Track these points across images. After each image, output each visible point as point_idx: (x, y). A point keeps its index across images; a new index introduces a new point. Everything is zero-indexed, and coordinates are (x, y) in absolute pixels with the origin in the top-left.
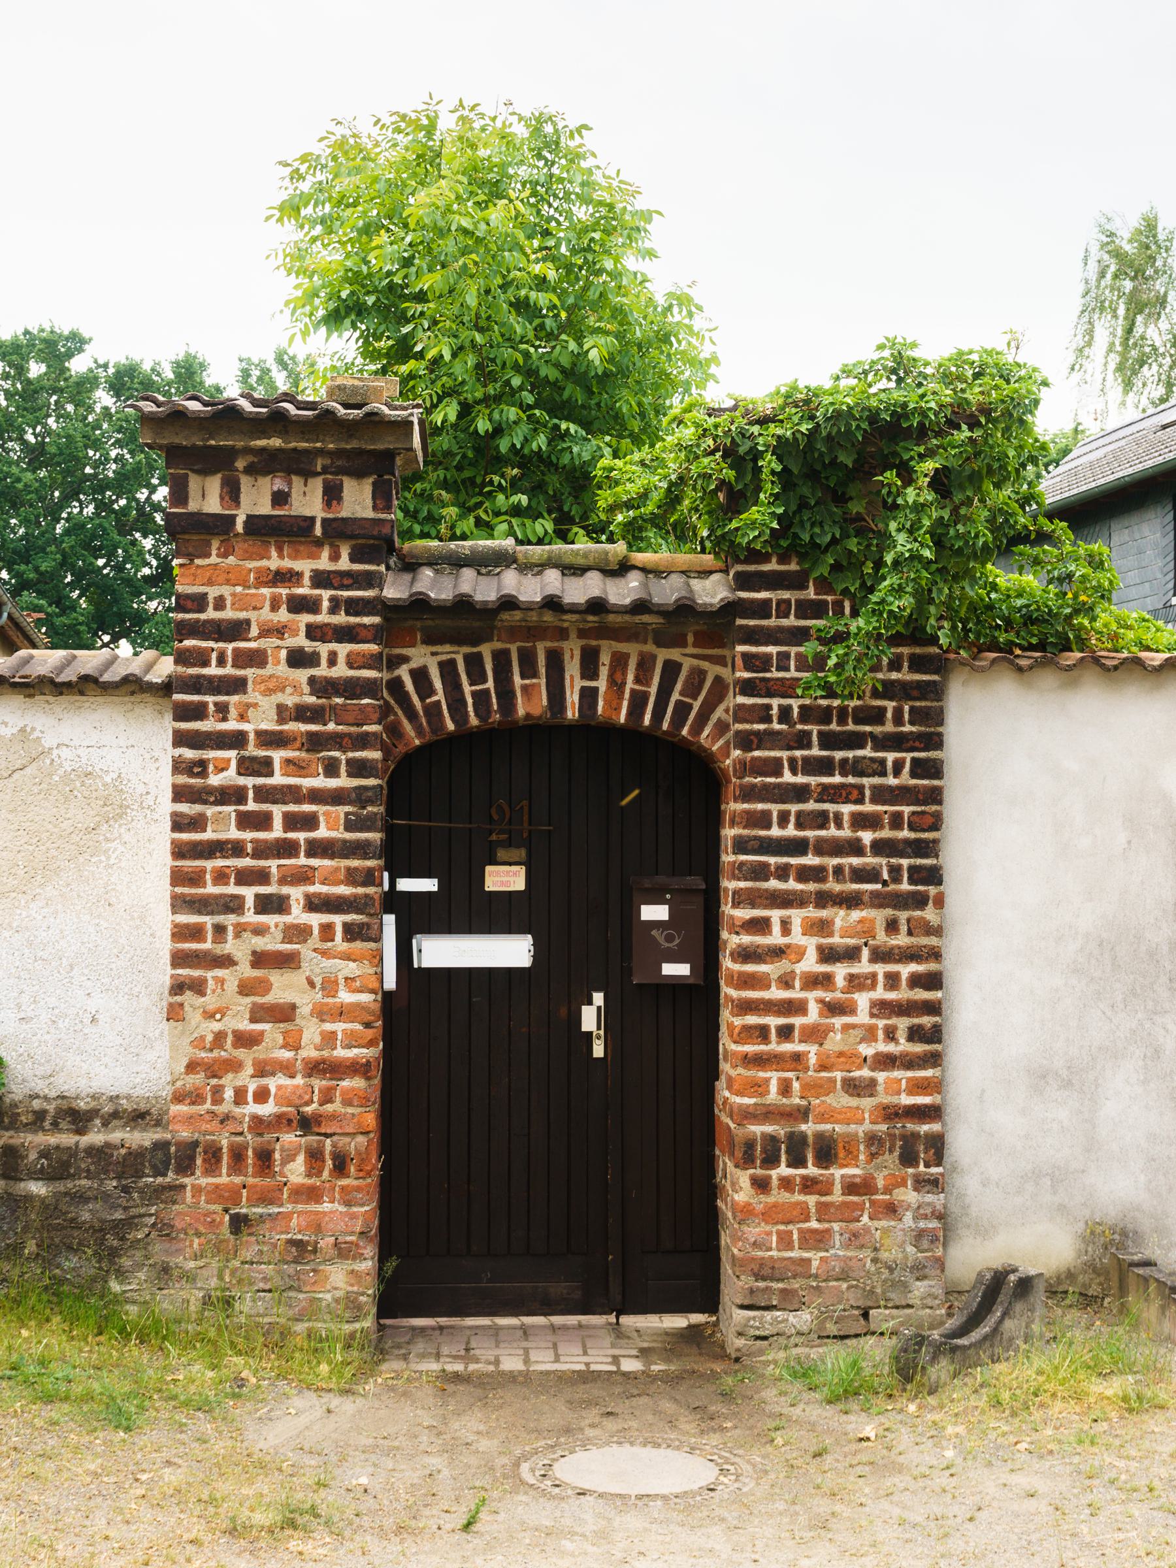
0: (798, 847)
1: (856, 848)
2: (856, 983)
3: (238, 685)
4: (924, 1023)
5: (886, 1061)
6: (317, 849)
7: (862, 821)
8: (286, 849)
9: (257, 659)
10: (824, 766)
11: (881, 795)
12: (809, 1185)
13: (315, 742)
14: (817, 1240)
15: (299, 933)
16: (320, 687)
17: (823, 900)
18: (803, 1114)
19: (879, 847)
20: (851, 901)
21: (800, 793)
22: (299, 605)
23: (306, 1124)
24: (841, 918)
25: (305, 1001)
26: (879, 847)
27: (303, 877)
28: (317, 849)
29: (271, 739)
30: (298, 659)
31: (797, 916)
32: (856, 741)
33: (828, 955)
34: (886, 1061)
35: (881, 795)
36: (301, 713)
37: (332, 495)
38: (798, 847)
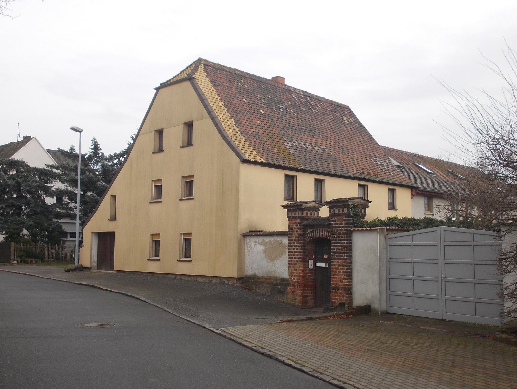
0: (336, 252)
1: (341, 253)
2: (341, 269)
3: (292, 234)
4: (349, 275)
5: (344, 279)
6: (299, 252)
7: (342, 250)
8: (296, 252)
9: (293, 232)
10: (338, 243)
11: (344, 246)
12: (336, 293)
13: (298, 240)
14: (336, 299)
15: (297, 261)
16: (299, 235)
17: (338, 259)
18: (337, 284)
19: (344, 253)
20: (340, 259)
21: (336, 246)
22: (297, 226)
23: (298, 282)
24: (340, 261)
25: (297, 269)
26: (344, 253)
27: (297, 255)
28: (299, 252)
29: (295, 240)
30: (297, 231)
31: (336, 261)
32: (341, 240)
33: (339, 265)
34: (344, 279)
35: (344, 246)
36: (297, 237)
37: (298, 214)
38: (336, 252)
